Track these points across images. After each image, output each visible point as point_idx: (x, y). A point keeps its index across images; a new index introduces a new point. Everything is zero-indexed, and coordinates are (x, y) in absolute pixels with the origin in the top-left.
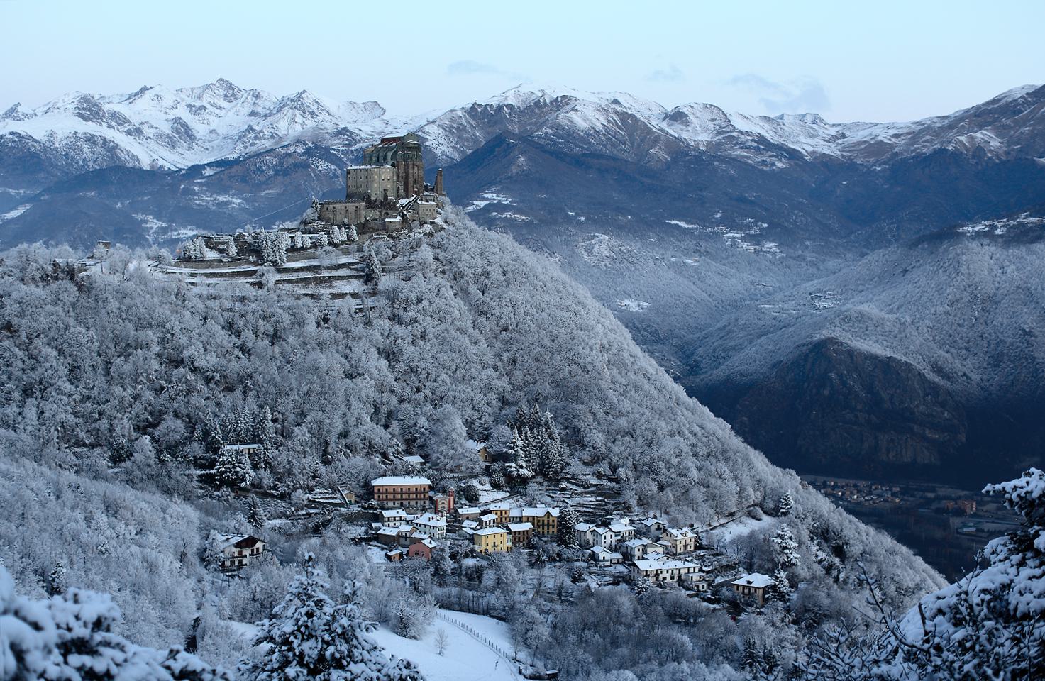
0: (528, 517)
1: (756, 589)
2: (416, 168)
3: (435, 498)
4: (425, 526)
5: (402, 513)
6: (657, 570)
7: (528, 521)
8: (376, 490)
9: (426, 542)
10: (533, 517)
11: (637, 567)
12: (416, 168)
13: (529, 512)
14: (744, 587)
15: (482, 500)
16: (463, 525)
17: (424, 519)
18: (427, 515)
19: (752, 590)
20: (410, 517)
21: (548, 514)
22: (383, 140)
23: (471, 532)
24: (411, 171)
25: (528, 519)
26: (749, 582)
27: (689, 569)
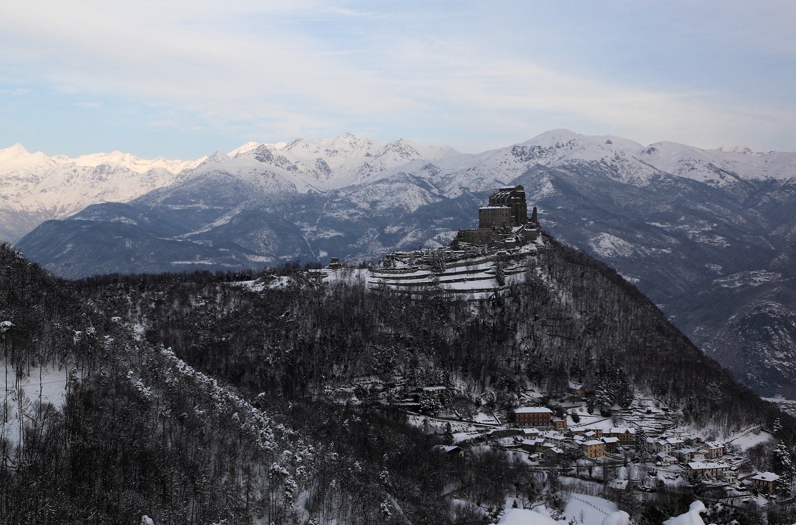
0: (614, 434)
1: (768, 482)
2: (523, 208)
3: (554, 421)
4: (552, 439)
5: (536, 431)
6: (702, 469)
7: (614, 436)
8: (518, 416)
9: (554, 449)
10: (618, 434)
11: (690, 467)
12: (523, 208)
13: (615, 430)
14: (760, 480)
15: (581, 422)
16: (574, 438)
17: (551, 434)
18: (552, 432)
19: (765, 484)
20: (541, 433)
21: (627, 432)
22: (501, 190)
23: (580, 443)
24: (519, 209)
25: (615, 435)
26: (763, 478)
27: (722, 468)
